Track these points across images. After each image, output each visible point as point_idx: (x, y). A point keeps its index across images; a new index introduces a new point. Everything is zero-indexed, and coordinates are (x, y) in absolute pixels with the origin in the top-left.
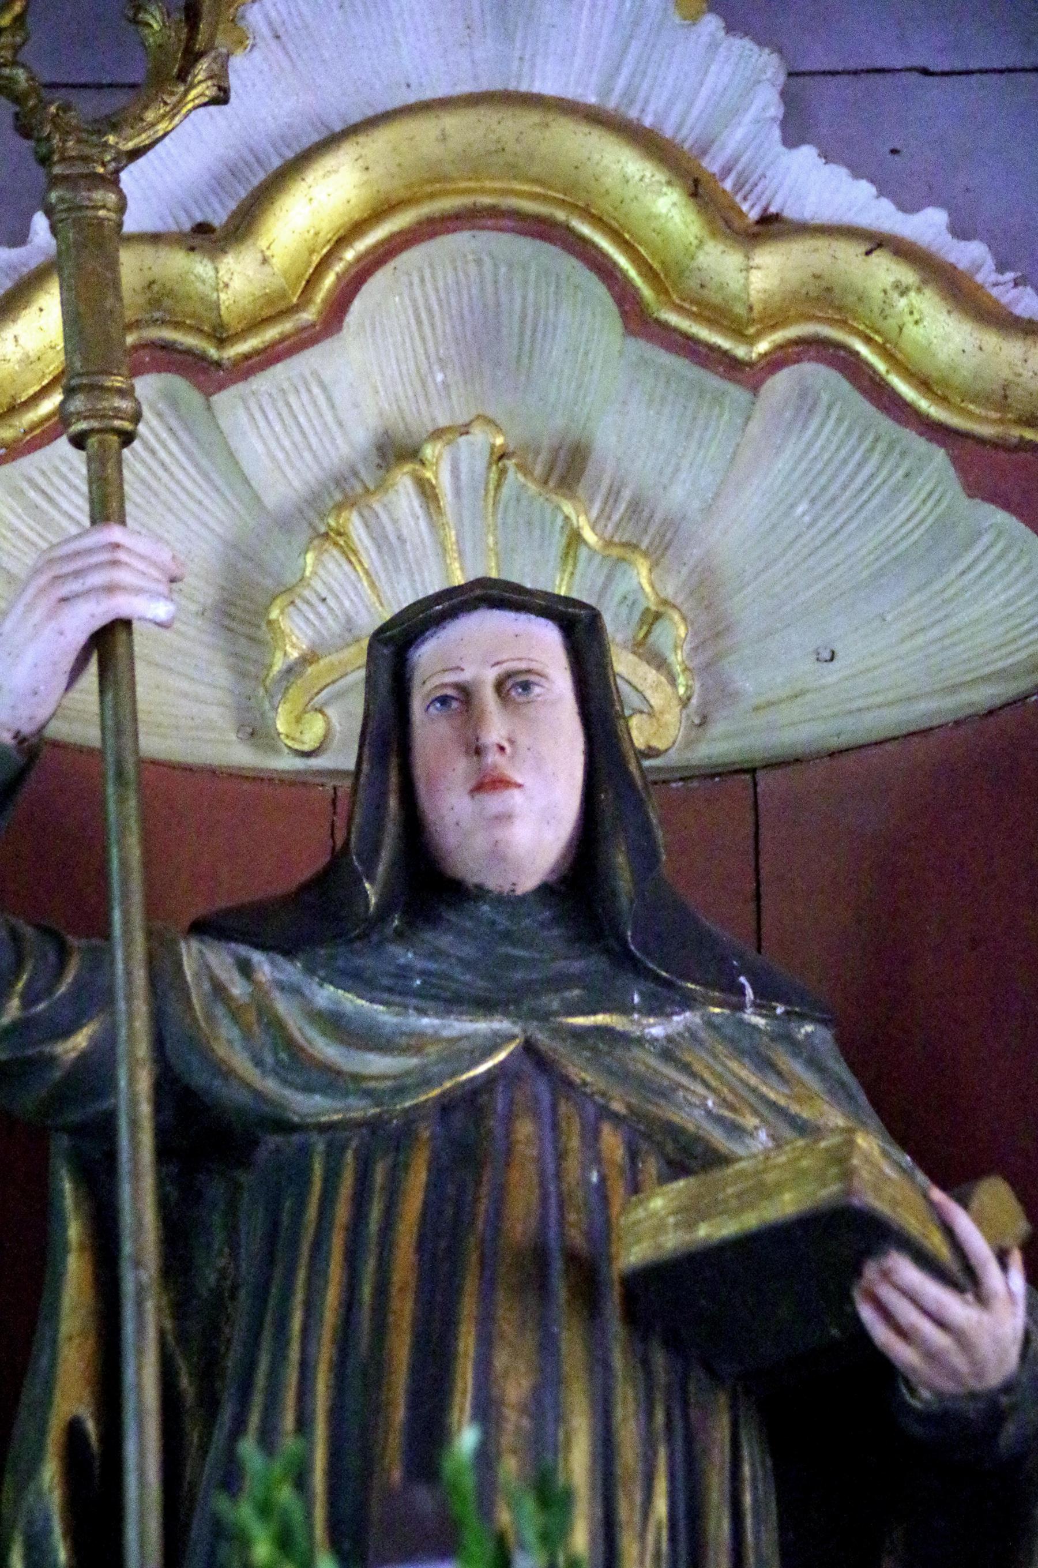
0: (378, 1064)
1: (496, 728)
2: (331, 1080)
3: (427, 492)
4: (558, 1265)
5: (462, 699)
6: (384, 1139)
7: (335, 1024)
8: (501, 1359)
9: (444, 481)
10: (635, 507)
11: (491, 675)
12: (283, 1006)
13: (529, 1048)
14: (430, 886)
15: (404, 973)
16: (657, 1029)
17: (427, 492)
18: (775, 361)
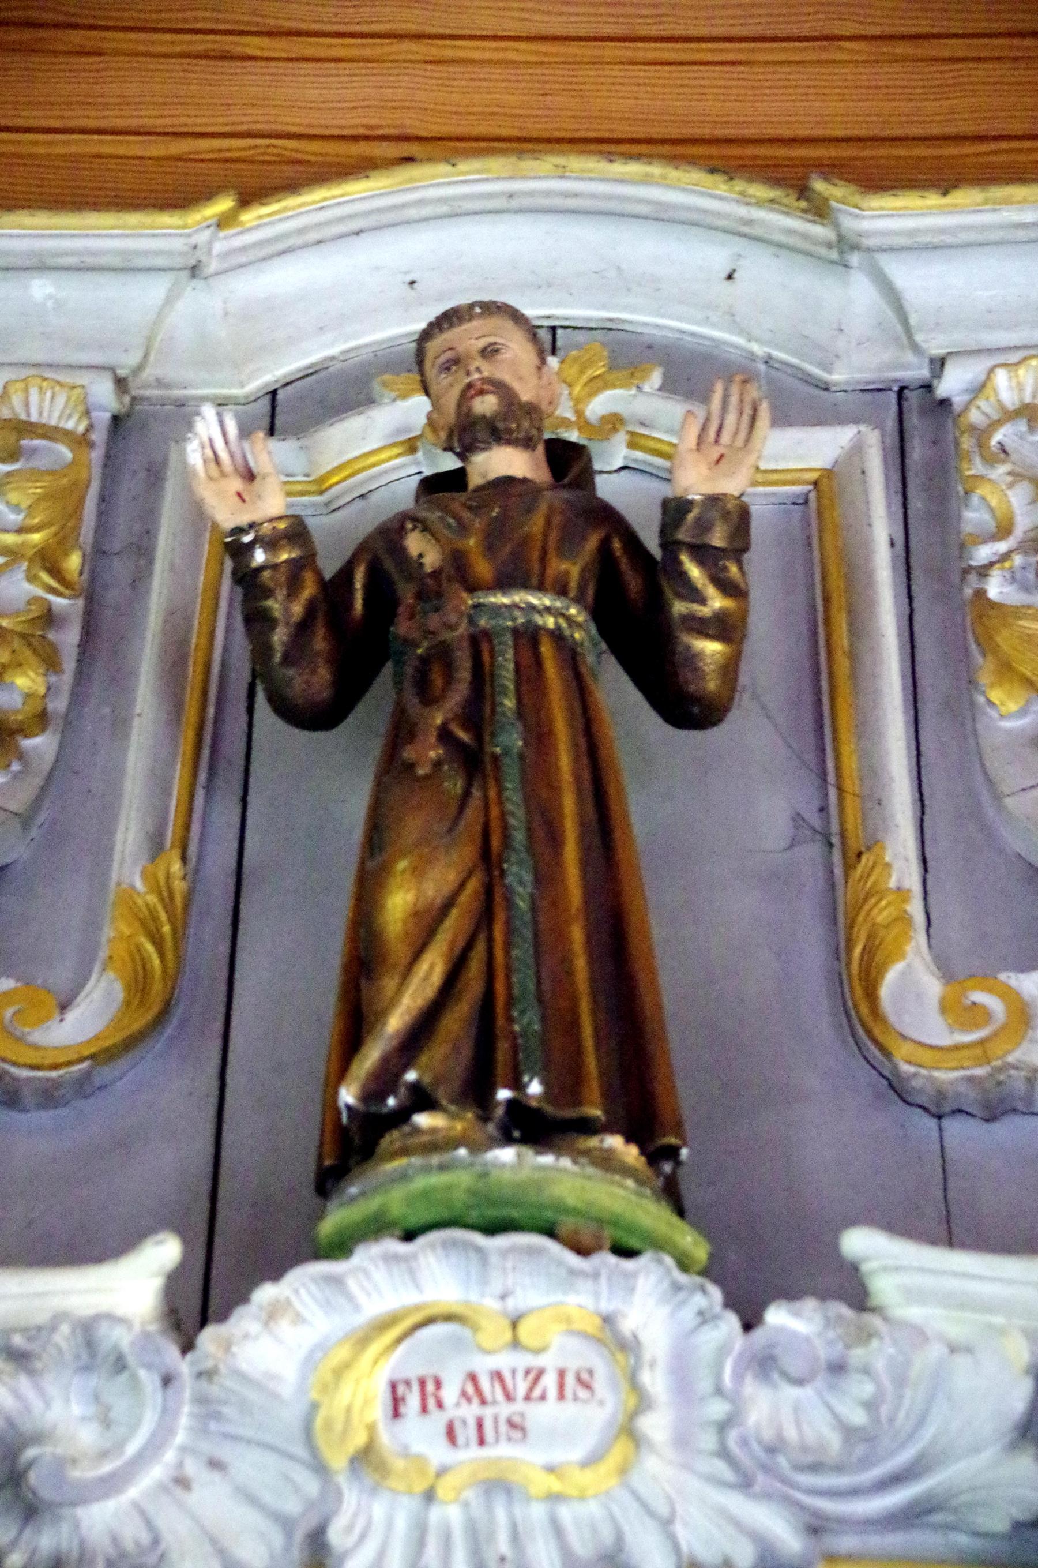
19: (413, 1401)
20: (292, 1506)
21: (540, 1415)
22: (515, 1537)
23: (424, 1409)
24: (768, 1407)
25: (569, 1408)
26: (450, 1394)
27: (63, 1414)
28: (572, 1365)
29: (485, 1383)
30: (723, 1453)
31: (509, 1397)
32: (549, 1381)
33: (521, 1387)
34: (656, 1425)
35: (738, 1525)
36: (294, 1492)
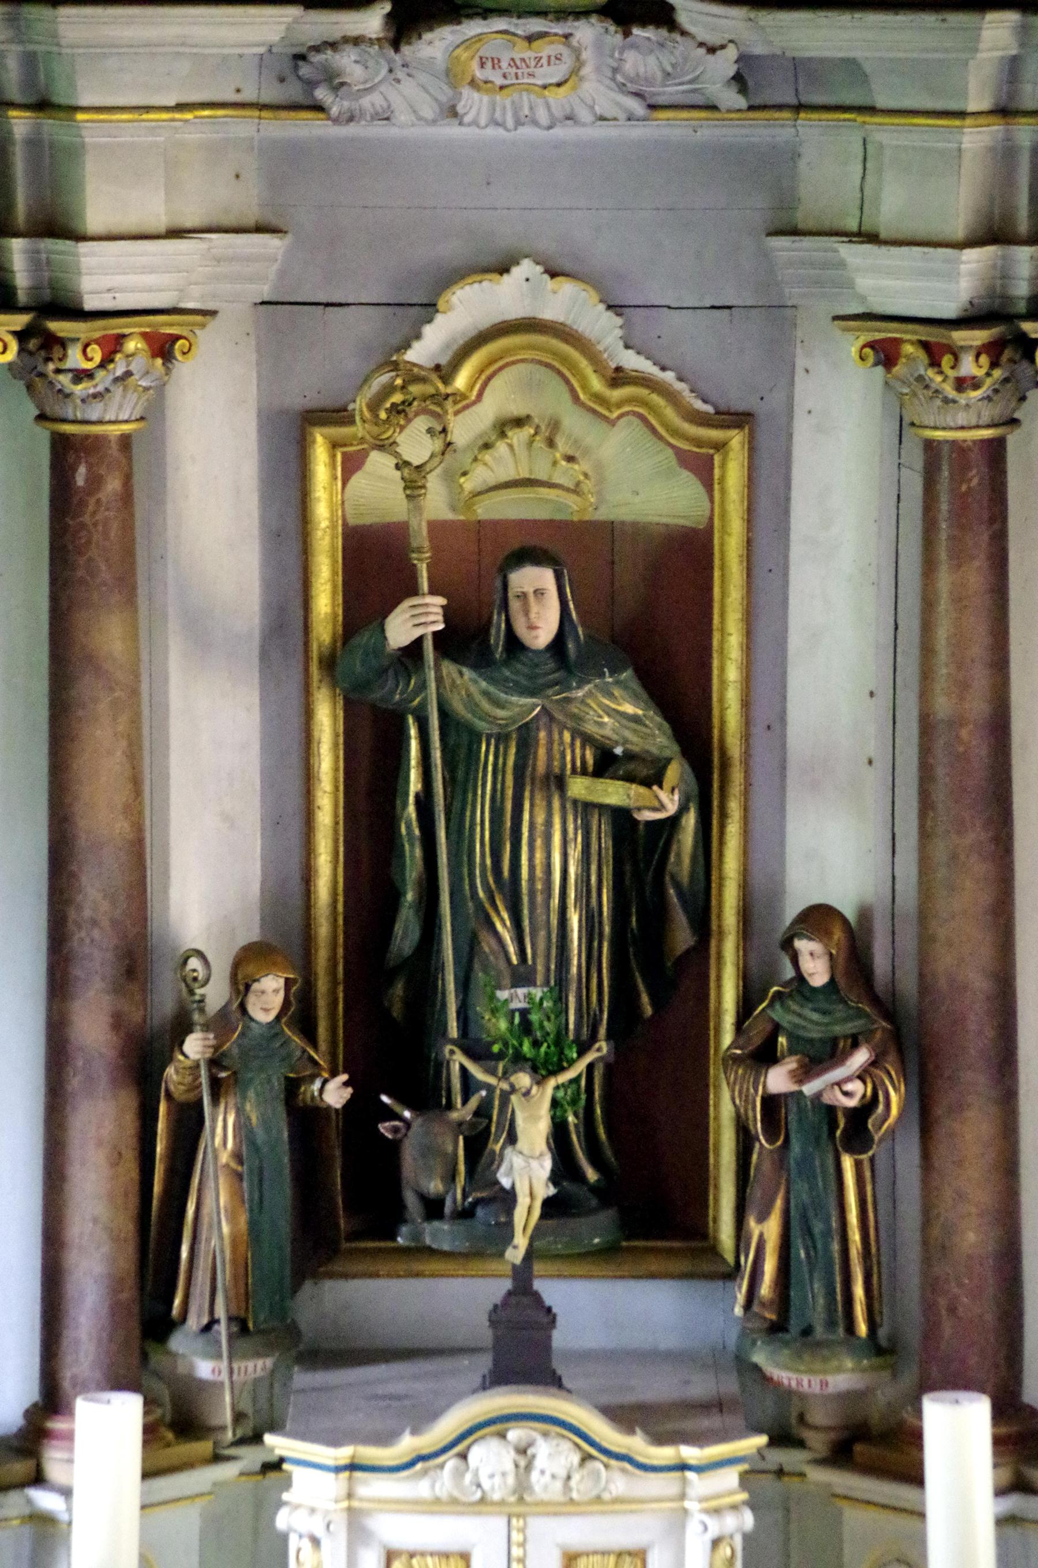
0: (501, 713)
1: (534, 608)
2: (485, 717)
3: (511, 446)
4: (552, 778)
5: (523, 596)
6: (502, 739)
7: (486, 694)
8: (537, 809)
9: (515, 441)
10: (576, 441)
11: (531, 590)
12: (473, 689)
13: (543, 708)
14: (514, 644)
15: (506, 680)
16: (580, 694)
17: (511, 446)
18: (620, 417)
19: (489, 64)
20: (443, 99)
21: (538, 71)
22: (531, 108)
23: (493, 67)
24: (633, 62)
25: (552, 68)
26: (504, 64)
27: (347, 61)
28: (553, 54)
29: (518, 63)
30: (613, 79)
31: (528, 67)
32: (544, 61)
33: (533, 63)
34: (587, 70)
35: (618, 104)
36: (445, 94)
